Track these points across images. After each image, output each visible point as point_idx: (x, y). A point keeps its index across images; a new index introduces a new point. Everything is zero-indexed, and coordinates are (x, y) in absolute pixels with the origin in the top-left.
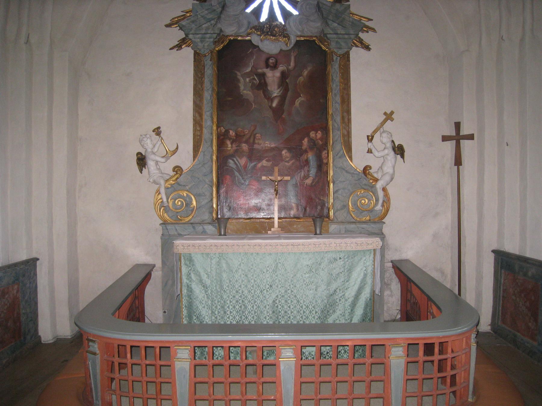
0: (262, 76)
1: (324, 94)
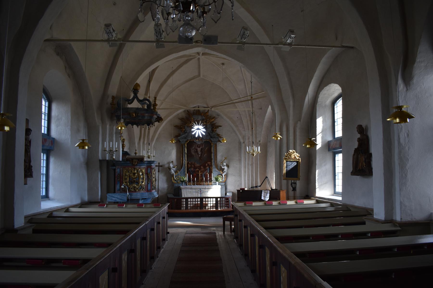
0: (197, 149)
1: (211, 153)
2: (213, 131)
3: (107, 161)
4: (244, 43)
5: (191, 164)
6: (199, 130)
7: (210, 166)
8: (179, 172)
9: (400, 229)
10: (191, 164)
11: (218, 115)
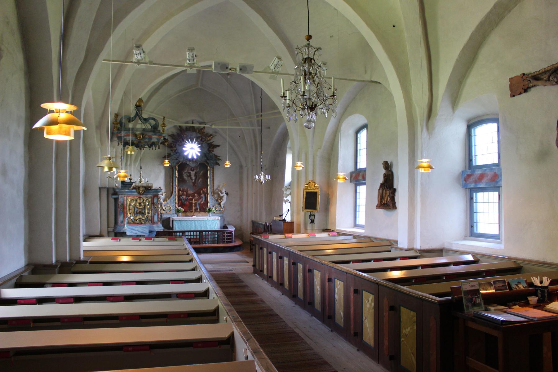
0: (190, 173)
2: (210, 151)
3: (108, 189)
4: (278, 73)
5: (183, 191)
6: (192, 150)
7: (206, 194)
8: (168, 201)
9: (419, 254)
10: (183, 191)
11: (216, 132)
